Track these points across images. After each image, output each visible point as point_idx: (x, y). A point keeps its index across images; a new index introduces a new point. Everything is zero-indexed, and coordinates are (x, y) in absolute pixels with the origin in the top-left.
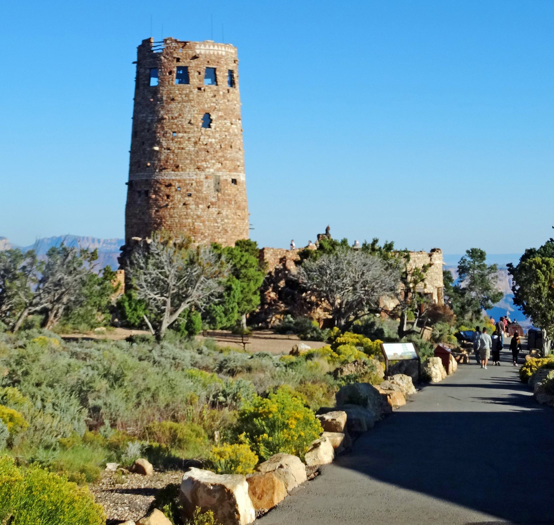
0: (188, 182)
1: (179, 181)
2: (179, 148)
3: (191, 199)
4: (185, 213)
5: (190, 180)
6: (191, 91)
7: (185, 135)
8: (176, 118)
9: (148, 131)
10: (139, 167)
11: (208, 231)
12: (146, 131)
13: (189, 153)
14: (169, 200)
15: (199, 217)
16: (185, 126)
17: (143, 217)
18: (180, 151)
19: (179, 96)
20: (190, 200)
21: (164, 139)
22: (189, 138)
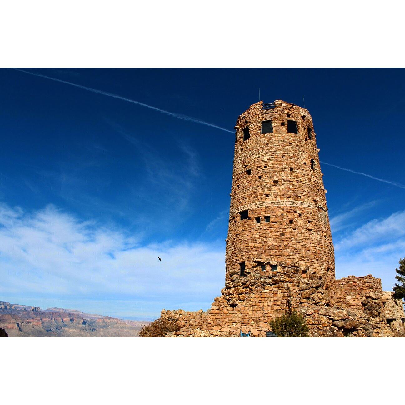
0: (307, 210)
1: (300, 209)
2: (298, 182)
3: (311, 225)
4: (308, 238)
5: (309, 209)
6: (301, 140)
7: (301, 171)
8: (292, 157)
9: (265, 167)
10: (257, 197)
11: (325, 257)
12: (263, 167)
13: (305, 186)
14: (292, 225)
15: (319, 243)
16: (300, 165)
17: (265, 240)
18: (298, 183)
19: (293, 141)
20: (311, 226)
21: (283, 173)
22: (304, 175)
